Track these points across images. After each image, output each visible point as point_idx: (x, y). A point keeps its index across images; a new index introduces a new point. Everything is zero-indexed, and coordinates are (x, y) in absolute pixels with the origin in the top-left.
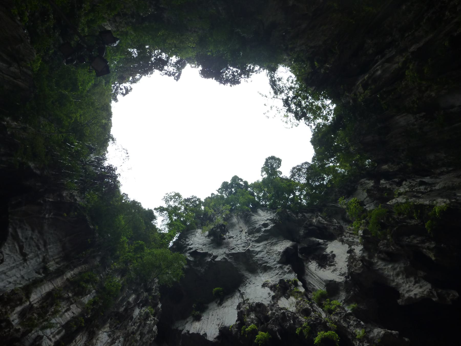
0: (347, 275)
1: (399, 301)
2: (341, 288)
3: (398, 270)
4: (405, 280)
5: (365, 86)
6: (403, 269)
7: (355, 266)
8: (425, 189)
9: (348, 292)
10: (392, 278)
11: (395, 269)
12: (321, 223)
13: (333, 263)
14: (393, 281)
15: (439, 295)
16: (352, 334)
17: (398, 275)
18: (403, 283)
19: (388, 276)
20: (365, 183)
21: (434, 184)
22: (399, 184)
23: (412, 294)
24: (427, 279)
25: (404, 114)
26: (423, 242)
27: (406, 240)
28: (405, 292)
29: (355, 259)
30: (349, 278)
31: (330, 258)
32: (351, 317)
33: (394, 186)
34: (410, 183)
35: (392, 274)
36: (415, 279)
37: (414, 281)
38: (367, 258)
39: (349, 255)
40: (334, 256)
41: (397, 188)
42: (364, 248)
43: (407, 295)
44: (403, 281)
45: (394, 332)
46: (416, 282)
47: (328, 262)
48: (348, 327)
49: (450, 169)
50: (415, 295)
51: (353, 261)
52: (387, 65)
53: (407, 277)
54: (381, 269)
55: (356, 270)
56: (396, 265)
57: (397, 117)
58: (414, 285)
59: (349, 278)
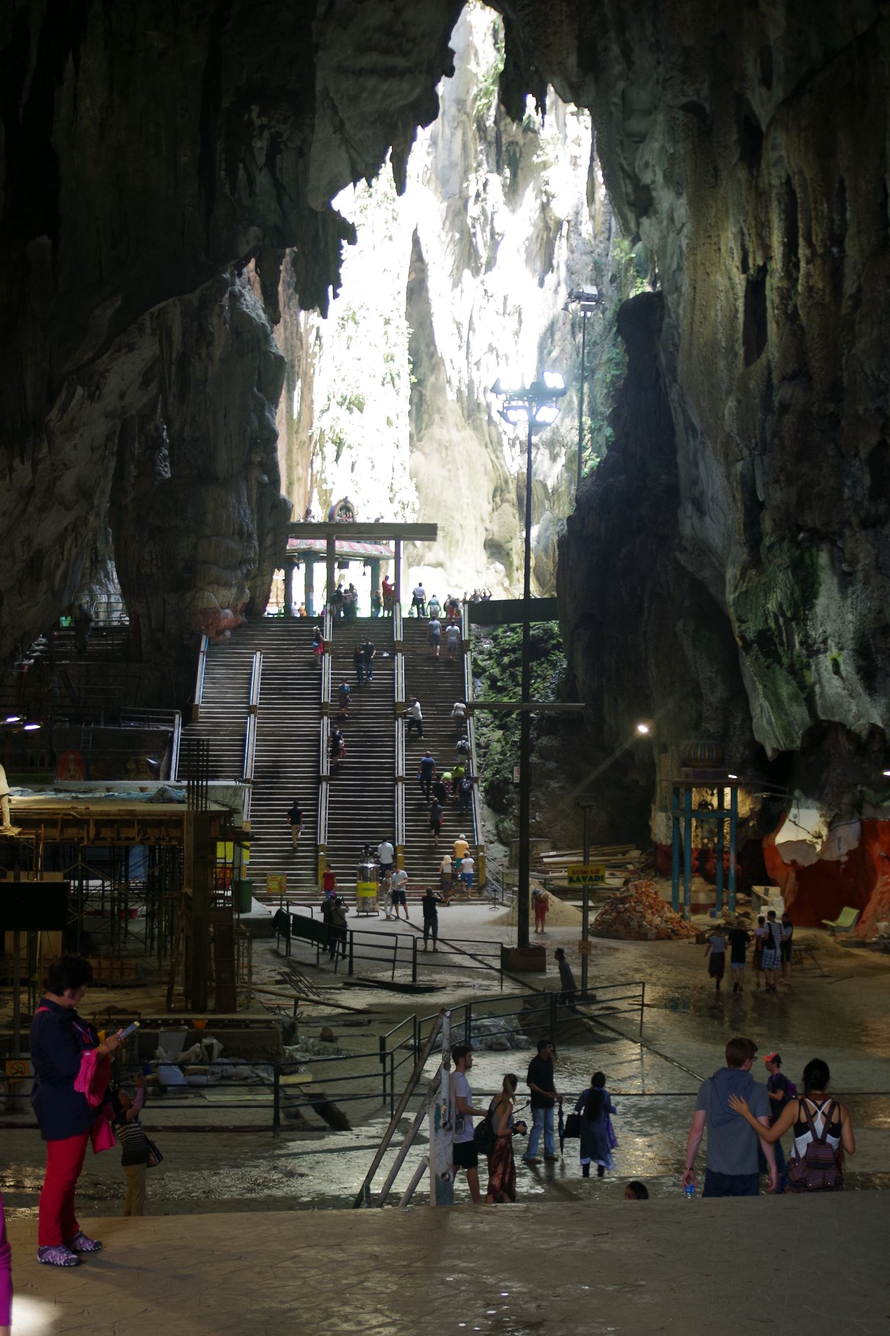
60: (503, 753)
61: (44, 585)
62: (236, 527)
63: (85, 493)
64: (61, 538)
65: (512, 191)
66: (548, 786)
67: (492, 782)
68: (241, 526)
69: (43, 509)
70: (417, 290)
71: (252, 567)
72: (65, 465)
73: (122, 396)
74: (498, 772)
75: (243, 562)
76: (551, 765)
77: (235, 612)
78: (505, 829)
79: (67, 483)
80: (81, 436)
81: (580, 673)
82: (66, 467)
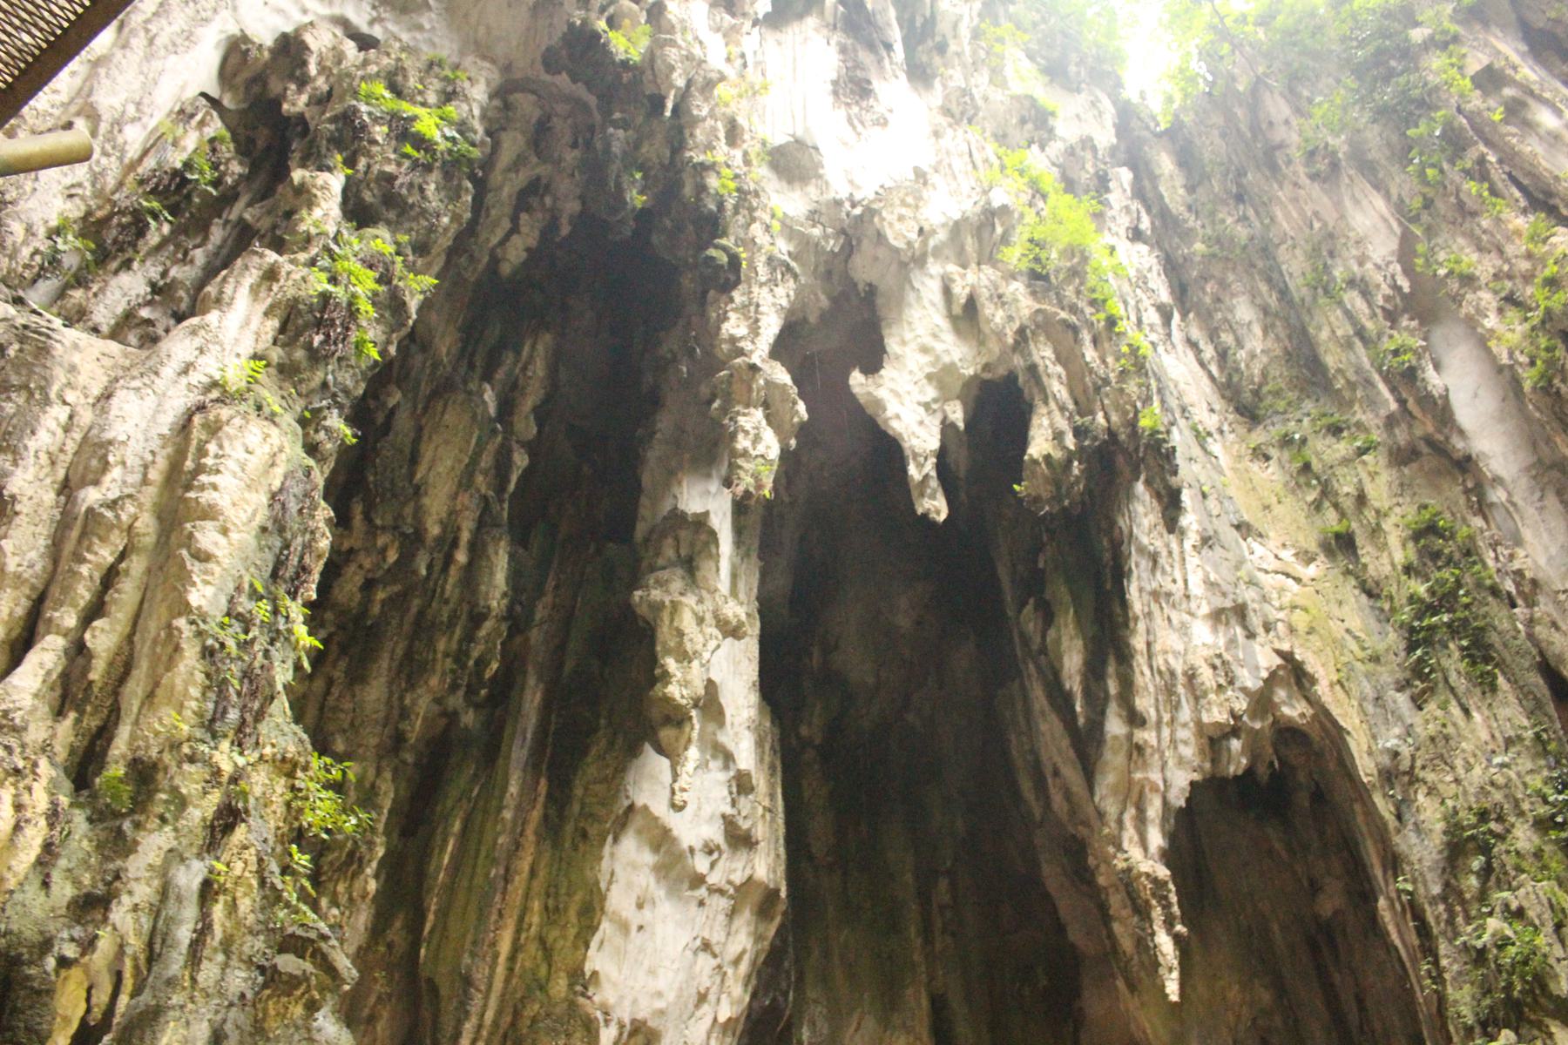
0: (857, 197)
1: (856, 379)
2: (812, 190)
3: (939, 347)
4: (921, 375)
5: (1490, 79)
6: (946, 359)
7: (901, 218)
8: (1151, 326)
9: (814, 216)
10: (908, 336)
11: (935, 336)
12: (955, 26)
13: (860, 128)
14: (903, 343)
15: (926, 477)
16: (750, 299)
17: (925, 350)
18: (911, 372)
19: (910, 323)
20: (1100, 114)
21: (1174, 347)
22: (1136, 235)
23: (892, 408)
24: (947, 427)
25: (1395, 225)
26: (1062, 409)
27: (1043, 353)
28: (892, 385)
29: (917, 207)
30: (854, 206)
31: (869, 109)
32: (791, 283)
33: (1125, 221)
34: (1150, 269)
35: (918, 332)
36: (935, 401)
37: (928, 399)
38: (932, 243)
39: (912, 177)
40: (882, 122)
41: (1122, 232)
42: (956, 223)
43: (882, 393)
44: (916, 369)
45: (801, 407)
46: (927, 406)
47: (855, 109)
48: (761, 285)
49: (1214, 369)
50: (898, 417)
51: (908, 206)
53: (929, 377)
54: (919, 298)
55: (891, 224)
56: (949, 337)
57: (1379, 203)
58: (919, 404)
59: (854, 206)
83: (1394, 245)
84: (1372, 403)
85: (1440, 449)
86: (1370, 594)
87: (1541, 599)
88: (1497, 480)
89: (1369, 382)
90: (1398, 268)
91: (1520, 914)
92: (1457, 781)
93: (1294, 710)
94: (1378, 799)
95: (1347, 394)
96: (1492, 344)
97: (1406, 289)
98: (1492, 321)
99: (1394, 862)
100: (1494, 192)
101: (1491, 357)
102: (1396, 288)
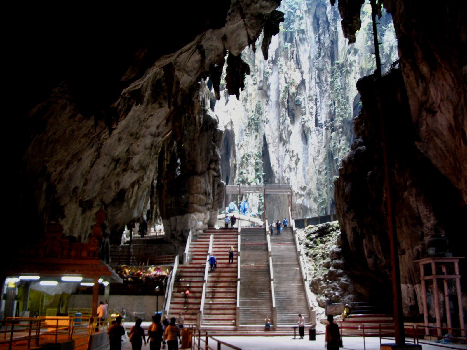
52: (308, 55)
60: (315, 269)
61: (125, 204)
62: (204, 191)
63: (143, 168)
64: (133, 185)
65: (293, 122)
66: (339, 280)
67: (313, 281)
68: (206, 190)
69: (125, 170)
70: (265, 155)
71: (210, 206)
72: (133, 153)
73: (158, 127)
74: (315, 276)
75: (207, 204)
76: (340, 271)
77: (203, 223)
78: (321, 300)
79: (135, 160)
80: (141, 141)
81: (349, 233)
82: (135, 154)
83: (276, 48)
84: (260, 76)
85: (266, 92)
86: (246, 111)
87: (268, 123)
88: (271, 100)
89: (260, 72)
90: (274, 53)
91: (248, 170)
92: (247, 149)
93: (229, 128)
94: (236, 147)
95: (256, 70)
96: (280, 85)
97: (274, 59)
98: (281, 81)
99: (235, 156)
100: (293, 58)
101: (279, 87)
102: (272, 58)
